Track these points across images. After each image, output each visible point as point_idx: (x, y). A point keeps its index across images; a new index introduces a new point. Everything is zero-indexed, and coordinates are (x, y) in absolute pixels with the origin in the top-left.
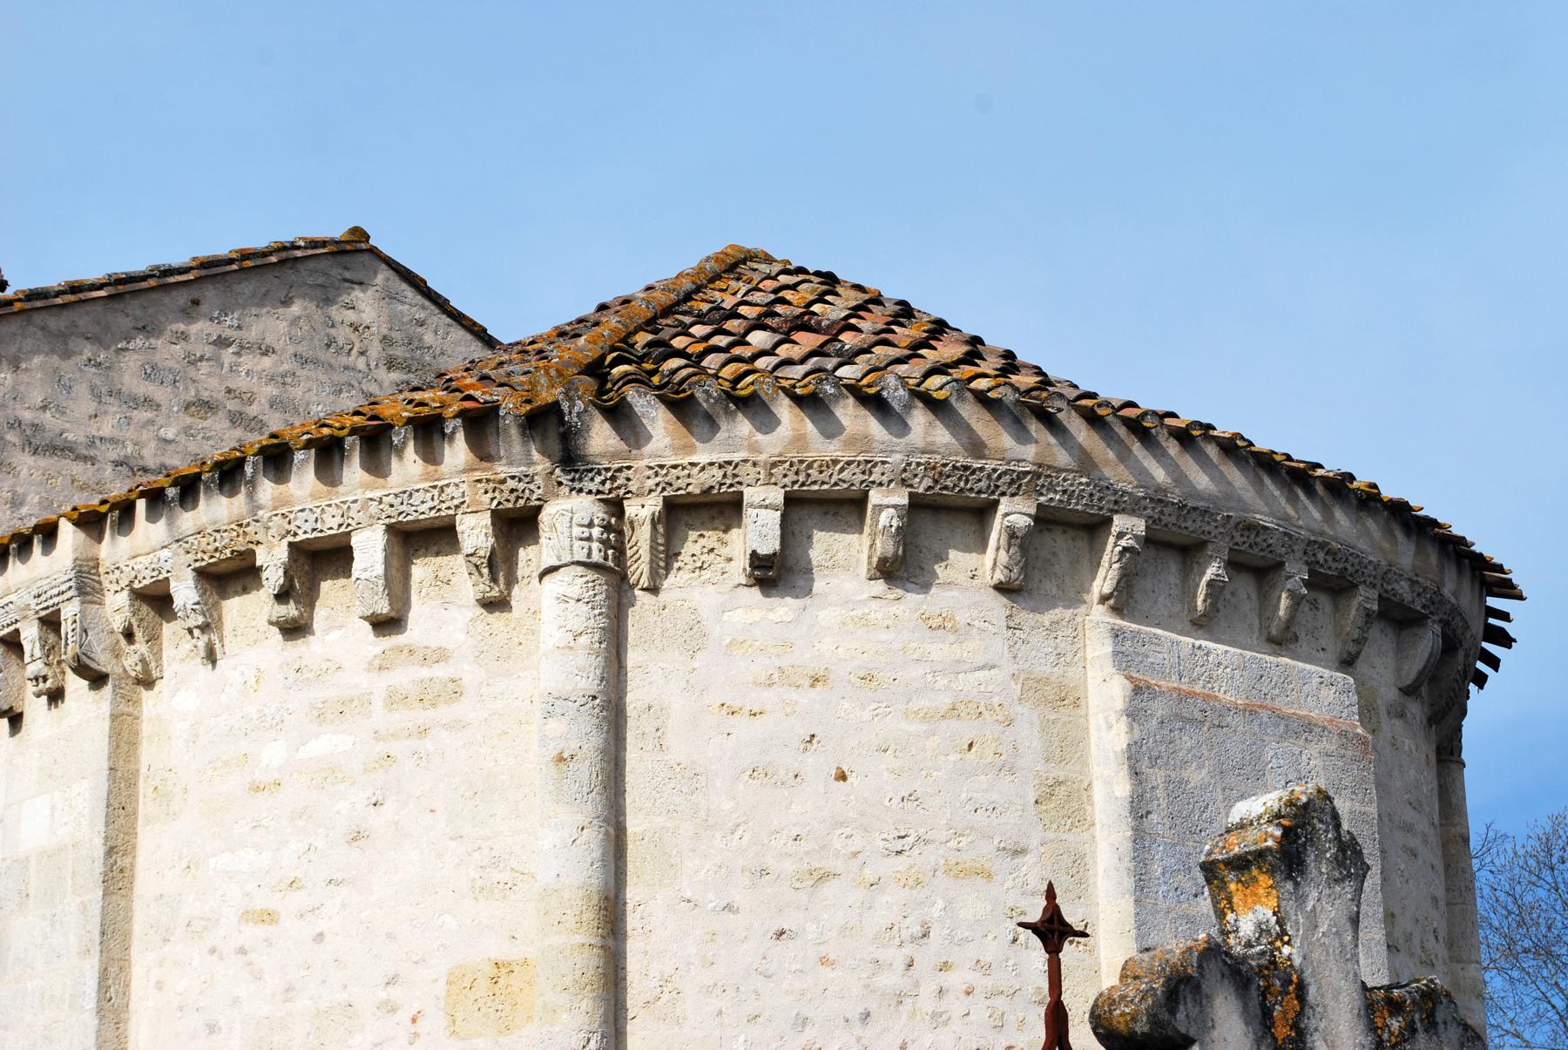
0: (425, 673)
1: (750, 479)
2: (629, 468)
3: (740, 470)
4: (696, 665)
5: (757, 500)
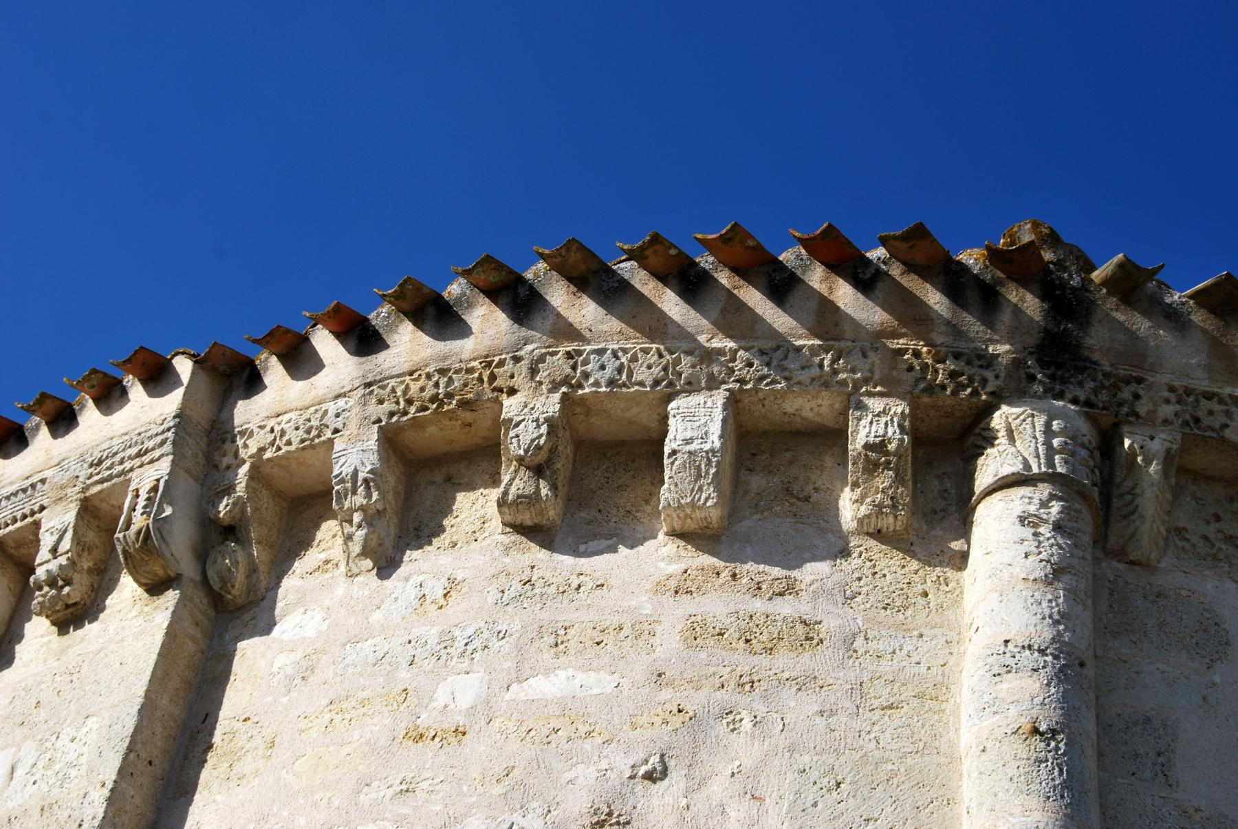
0: (758, 605)
2: (1140, 381)
4: (1217, 679)
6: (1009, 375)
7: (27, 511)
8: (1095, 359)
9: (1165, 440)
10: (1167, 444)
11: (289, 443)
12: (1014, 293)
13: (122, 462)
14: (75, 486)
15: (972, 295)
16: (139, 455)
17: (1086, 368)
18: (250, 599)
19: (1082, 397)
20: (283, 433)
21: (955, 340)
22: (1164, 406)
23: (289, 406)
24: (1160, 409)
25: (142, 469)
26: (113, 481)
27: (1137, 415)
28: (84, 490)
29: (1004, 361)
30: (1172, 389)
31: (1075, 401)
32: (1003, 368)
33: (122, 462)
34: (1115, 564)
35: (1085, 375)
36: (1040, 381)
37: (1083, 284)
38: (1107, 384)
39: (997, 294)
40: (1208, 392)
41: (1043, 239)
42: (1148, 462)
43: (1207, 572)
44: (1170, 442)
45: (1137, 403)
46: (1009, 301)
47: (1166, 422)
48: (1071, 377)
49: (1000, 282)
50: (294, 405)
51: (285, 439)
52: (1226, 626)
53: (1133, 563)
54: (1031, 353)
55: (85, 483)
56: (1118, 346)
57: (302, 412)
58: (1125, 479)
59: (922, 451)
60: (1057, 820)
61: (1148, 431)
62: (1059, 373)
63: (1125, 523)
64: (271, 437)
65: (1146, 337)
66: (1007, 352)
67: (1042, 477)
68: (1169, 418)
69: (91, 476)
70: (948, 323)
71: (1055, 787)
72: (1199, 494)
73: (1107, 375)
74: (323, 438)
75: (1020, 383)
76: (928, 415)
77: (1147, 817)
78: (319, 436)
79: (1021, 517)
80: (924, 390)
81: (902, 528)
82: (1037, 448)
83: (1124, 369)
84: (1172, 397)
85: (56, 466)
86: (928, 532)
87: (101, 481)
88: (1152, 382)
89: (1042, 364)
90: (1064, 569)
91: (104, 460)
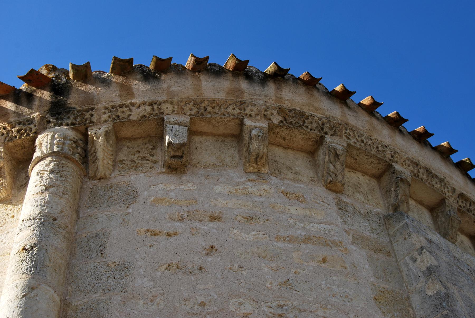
1: (169, 111)
2: (92, 109)
3: (164, 107)
4: (130, 211)
5: (172, 120)
6: (39, 124)
8: (73, 107)
9: (105, 128)
10: (106, 129)
12: (39, 93)
15: (24, 99)
17: (70, 111)
19: (69, 122)
21: (18, 118)
22: (103, 115)
24: (102, 117)
27: (93, 122)
29: (37, 119)
30: (106, 108)
31: (67, 125)
32: (37, 122)
34: (93, 181)
35: (70, 114)
36: (52, 122)
37: (67, 81)
38: (79, 115)
39: (33, 95)
40: (121, 105)
41: (50, 70)
42: (98, 138)
43: (132, 173)
44: (108, 128)
45: (92, 118)
46: (37, 96)
47: (106, 121)
48: (65, 116)
49: (34, 91)
52: (138, 190)
53: (100, 179)
54: (48, 113)
56: (81, 99)
58: (92, 148)
59: (21, 166)
60: (25, 281)
61: (99, 127)
62: (60, 116)
63: (94, 164)
65: (93, 92)
66: (38, 115)
67: (47, 155)
68: (106, 119)
70: (15, 112)
71: (27, 268)
72: (131, 146)
73: (78, 111)
75: (44, 125)
76: (17, 150)
77: (91, 272)
79: (38, 173)
80: (9, 140)
81: (6, 195)
82: (47, 146)
83: (85, 107)
84: (106, 111)
86: (18, 194)
88: (97, 108)
89: (52, 115)
90: (51, 186)
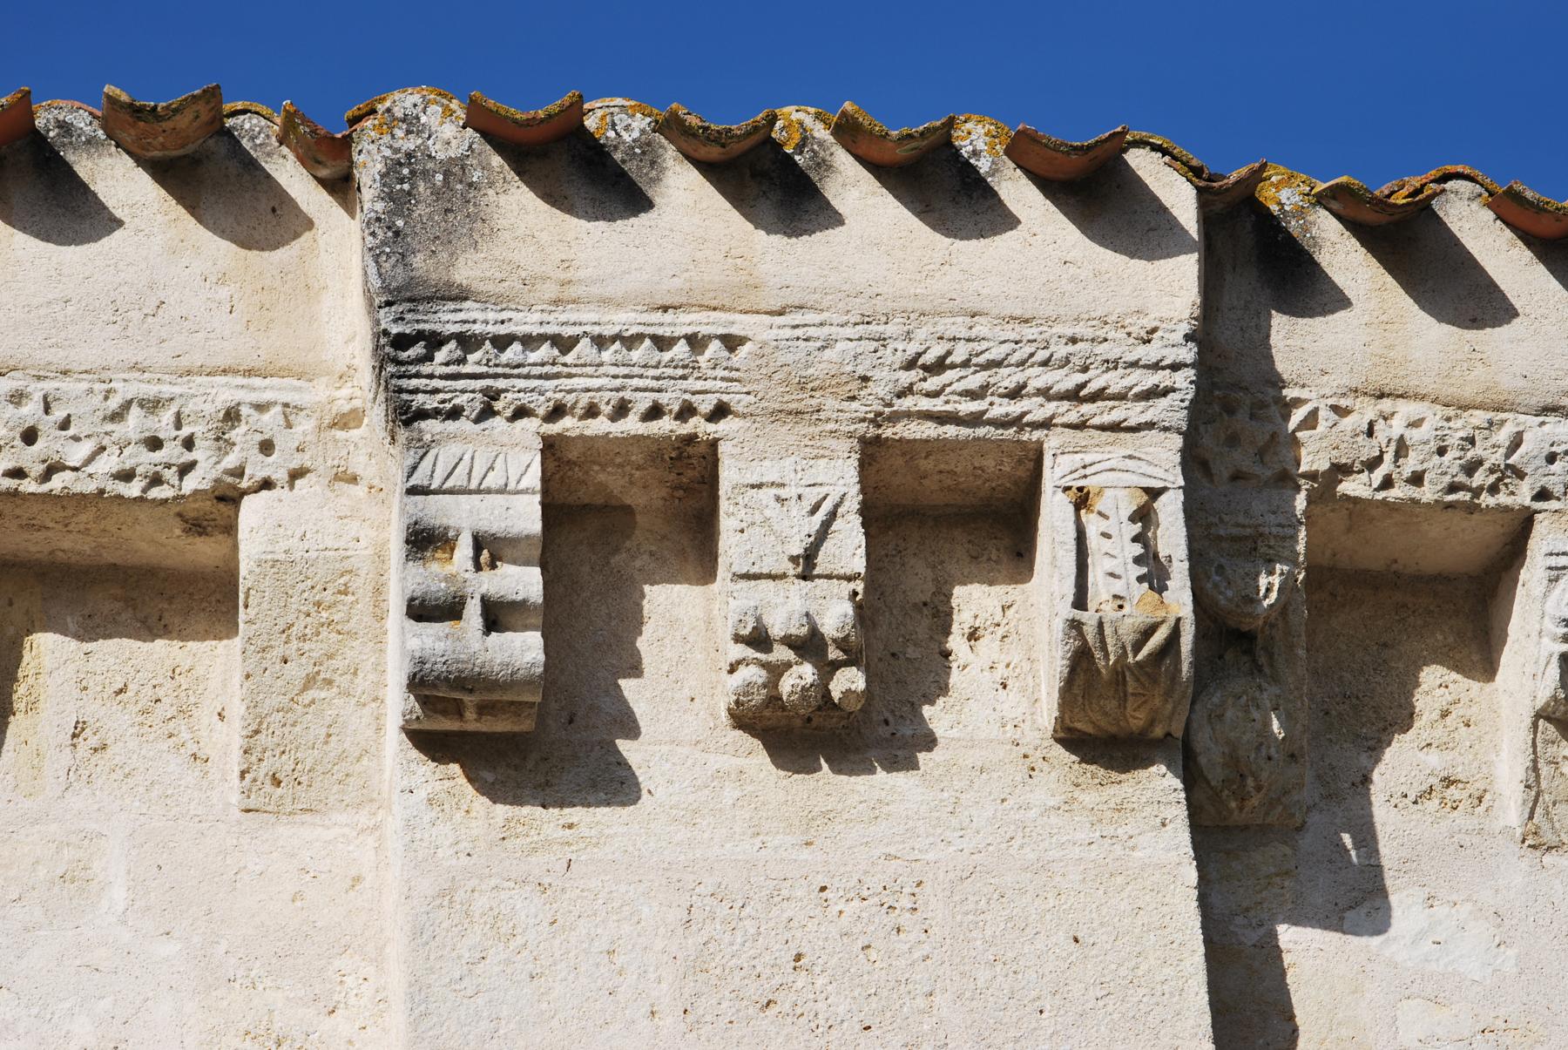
7: (671, 399)
11: (1417, 479)
13: (1015, 394)
14: (853, 398)
16: (1074, 396)
18: (1269, 820)
20: (1402, 449)
23: (1412, 383)
25: (1078, 434)
26: (981, 431)
28: (877, 420)
33: (1015, 394)
50: (1428, 385)
51: (1410, 465)
55: (890, 405)
57: (1451, 412)
64: (1368, 450)
69: (907, 391)
74: (1503, 498)
78: (1493, 489)
85: (771, 313)
87: (942, 419)
91: (953, 366)
